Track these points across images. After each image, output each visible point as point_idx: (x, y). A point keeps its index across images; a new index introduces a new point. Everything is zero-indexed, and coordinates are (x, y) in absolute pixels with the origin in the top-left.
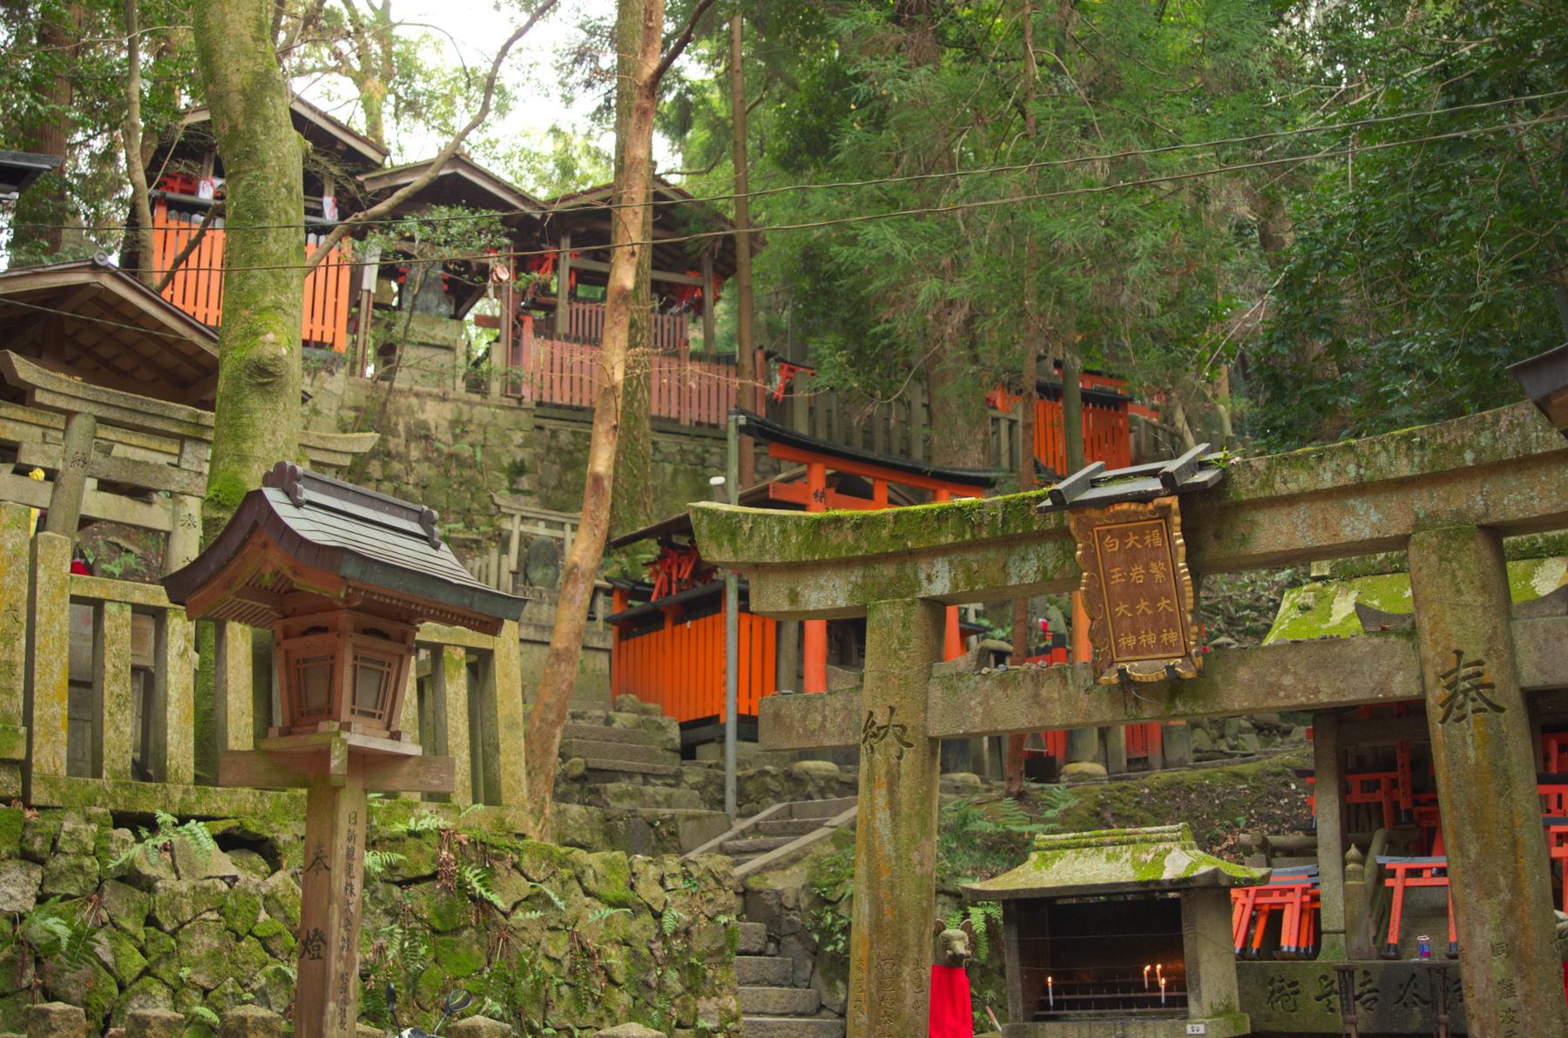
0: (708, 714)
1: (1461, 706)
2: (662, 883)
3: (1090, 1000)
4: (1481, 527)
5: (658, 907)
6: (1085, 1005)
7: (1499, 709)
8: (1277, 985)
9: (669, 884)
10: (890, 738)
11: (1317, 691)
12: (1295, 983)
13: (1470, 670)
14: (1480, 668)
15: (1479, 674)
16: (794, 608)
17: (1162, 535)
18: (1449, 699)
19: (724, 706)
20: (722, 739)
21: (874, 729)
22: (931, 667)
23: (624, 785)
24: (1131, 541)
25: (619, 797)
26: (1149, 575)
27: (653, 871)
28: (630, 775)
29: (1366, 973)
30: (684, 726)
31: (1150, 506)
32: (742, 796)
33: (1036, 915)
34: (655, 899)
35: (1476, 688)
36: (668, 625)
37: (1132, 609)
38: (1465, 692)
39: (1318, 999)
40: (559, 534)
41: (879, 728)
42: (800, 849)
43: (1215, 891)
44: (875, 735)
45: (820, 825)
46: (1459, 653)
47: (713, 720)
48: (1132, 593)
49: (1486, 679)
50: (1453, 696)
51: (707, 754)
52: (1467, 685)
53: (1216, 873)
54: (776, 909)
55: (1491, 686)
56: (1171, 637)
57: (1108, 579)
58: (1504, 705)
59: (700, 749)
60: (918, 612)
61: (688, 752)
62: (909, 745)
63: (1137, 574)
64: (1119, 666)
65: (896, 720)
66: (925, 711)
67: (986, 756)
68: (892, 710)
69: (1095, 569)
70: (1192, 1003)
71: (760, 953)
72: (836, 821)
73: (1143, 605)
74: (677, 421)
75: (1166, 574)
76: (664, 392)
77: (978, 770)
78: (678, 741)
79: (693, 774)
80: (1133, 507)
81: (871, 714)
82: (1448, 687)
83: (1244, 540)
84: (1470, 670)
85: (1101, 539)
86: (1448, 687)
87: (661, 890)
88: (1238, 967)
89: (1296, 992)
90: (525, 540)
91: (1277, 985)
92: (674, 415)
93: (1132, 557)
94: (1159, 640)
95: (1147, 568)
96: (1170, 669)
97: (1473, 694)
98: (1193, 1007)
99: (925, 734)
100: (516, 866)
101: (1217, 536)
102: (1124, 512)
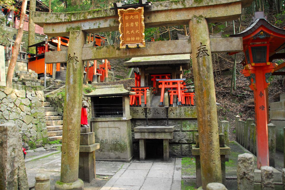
2: (31, 95)
3: (110, 114)
5: (31, 99)
6: (109, 114)
7: (208, 55)
8: (135, 111)
9: (33, 95)
12: (138, 111)
15: (205, 48)
17: (138, 16)
18: (199, 53)
19: (44, 72)
20: (44, 76)
21: (70, 58)
22: (84, 45)
24: (131, 17)
25: (28, 84)
26: (135, 25)
27: (30, 93)
29: (149, 109)
30: (38, 74)
31: (137, 9)
32: (47, 84)
33: (95, 99)
34: (30, 98)
36: (36, 60)
38: (202, 51)
39: (142, 113)
41: (71, 57)
44: (70, 59)
45: (58, 88)
46: (201, 43)
47: (43, 74)
48: (130, 29)
49: (206, 49)
50: (200, 52)
51: (42, 78)
52: (202, 50)
55: (207, 50)
56: (138, 38)
57: (125, 25)
60: (81, 33)
61: (39, 78)
63: (132, 25)
68: (75, 53)
69: (122, 23)
70: (124, 114)
71: (49, 106)
73: (132, 31)
74: (39, 34)
75: (139, 25)
78: (37, 76)
79: (40, 81)
86: (199, 50)
87: (31, 96)
88: (130, 108)
89: (138, 112)
91: (135, 111)
92: (39, 33)
94: (135, 39)
95: (134, 23)
96: (138, 45)
100: (3, 92)
101: (148, 18)
102: (129, 10)
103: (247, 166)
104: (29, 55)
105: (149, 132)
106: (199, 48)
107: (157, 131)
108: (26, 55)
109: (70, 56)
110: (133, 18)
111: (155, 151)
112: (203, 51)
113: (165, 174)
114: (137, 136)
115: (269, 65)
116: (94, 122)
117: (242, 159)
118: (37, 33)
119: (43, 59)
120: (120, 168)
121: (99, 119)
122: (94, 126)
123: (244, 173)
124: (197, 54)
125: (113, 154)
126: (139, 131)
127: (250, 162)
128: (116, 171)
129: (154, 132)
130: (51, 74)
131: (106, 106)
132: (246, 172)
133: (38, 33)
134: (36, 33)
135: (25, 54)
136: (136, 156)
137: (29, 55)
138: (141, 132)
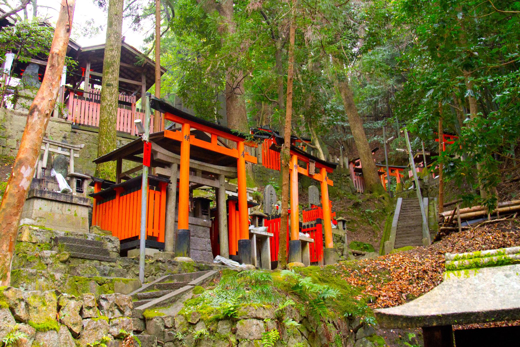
0: (134, 235)
2: (81, 313)
5: (76, 329)
19: (140, 231)
20: (138, 247)
30: (122, 242)
36: (117, 197)
42: (176, 296)
45: (185, 285)
54: (163, 328)
59: (129, 252)
67: (256, 259)
74: (130, 134)
76: (125, 124)
87: (79, 318)
90: (50, 154)
92: (129, 132)
104: (96, 185)
108: (86, 184)
118: (123, 132)
119: (136, 193)
130: (161, 240)
133: (125, 131)
134: (121, 130)
135: (83, 179)
137: (96, 185)
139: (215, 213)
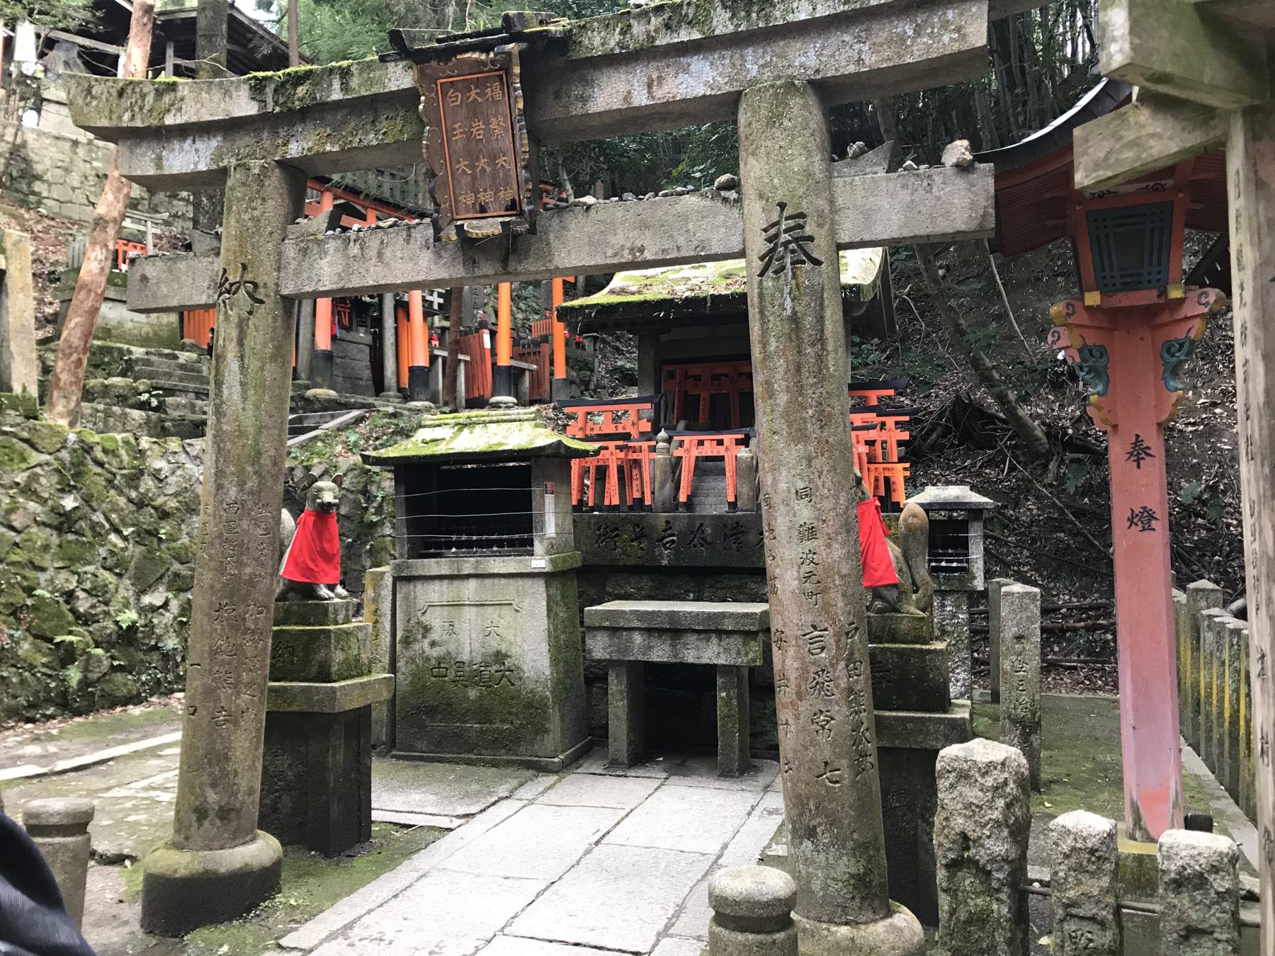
1: (782, 258)
4: (811, 83)
7: (817, 262)
10: (242, 292)
11: (642, 250)
13: (791, 223)
14: (801, 221)
16: (159, 172)
21: (227, 285)
23: (182, 400)
28: (185, 391)
35: (796, 240)
37: (473, 167)
38: (786, 244)
40: (142, 228)
41: (231, 285)
43: (557, 458)
44: (228, 292)
46: (782, 206)
53: (560, 442)
55: (811, 239)
58: (822, 258)
62: (262, 302)
64: (459, 223)
65: (249, 277)
66: (279, 270)
68: (244, 267)
70: (536, 543)
72: (325, 426)
77: (434, 399)
80: (476, 55)
81: (225, 271)
82: (769, 240)
83: (584, 100)
84: (791, 223)
85: (444, 95)
86: (769, 240)
93: (474, 112)
95: (487, 123)
97: (793, 246)
98: (538, 547)
99: (277, 292)
101: (557, 96)
103: (975, 801)
105: (649, 631)
106: (773, 231)
107: (685, 624)
109: (227, 280)
110: (480, 100)
111: (681, 722)
112: (789, 242)
113: (717, 832)
114: (599, 647)
115: (1181, 301)
116: (410, 579)
117: (956, 765)
120: (504, 795)
121: (432, 566)
122: (406, 598)
123: (964, 836)
124: (762, 258)
125: (475, 728)
126: (607, 624)
127: (989, 782)
128: (474, 809)
129: (674, 630)
131: (466, 506)
132: (973, 836)
136: (587, 746)
138: (615, 629)
139: (378, 322)
